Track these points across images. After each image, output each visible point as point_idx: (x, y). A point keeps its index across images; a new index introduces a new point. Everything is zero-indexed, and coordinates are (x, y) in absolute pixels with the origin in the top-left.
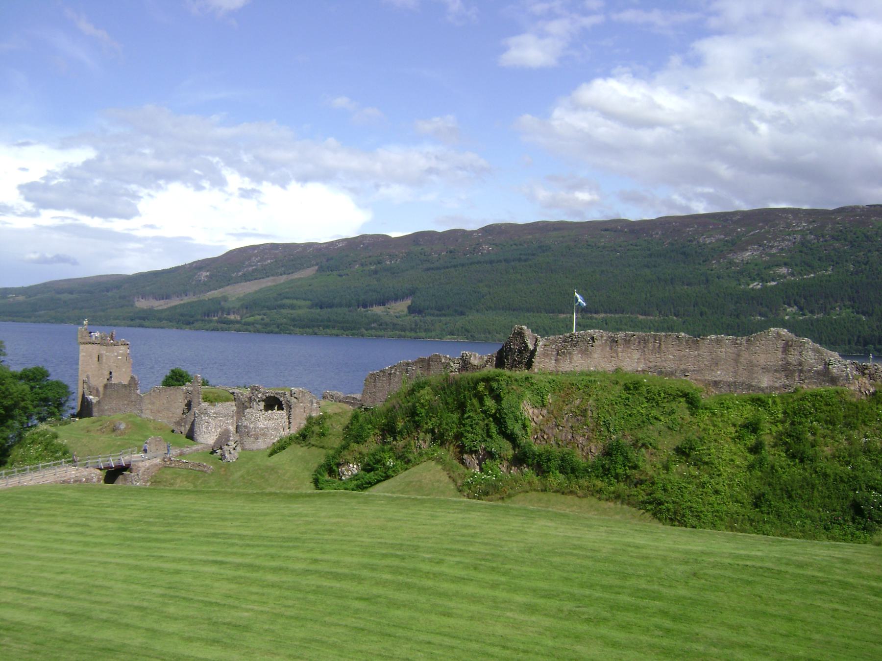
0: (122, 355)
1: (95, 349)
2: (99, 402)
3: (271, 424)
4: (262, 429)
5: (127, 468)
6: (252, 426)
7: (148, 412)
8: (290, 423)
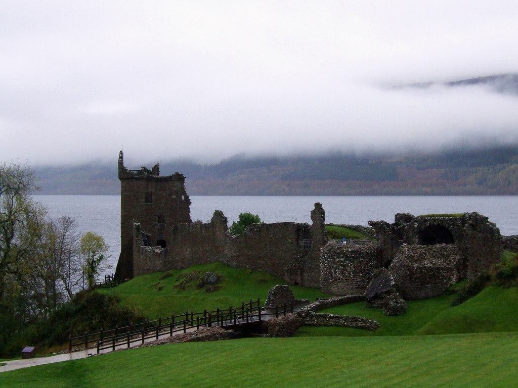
3: (440, 263)
4: (431, 269)
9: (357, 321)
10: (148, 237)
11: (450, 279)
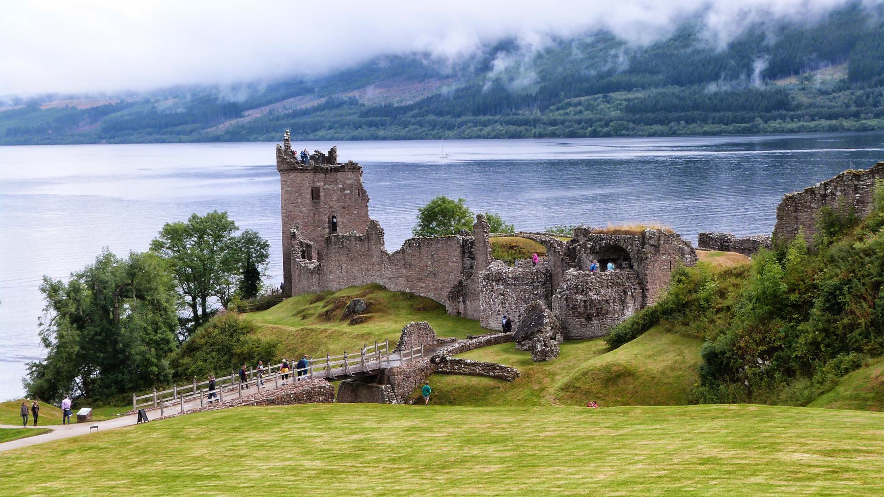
0: (351, 187)
2: (319, 269)
9: (495, 368)
10: (308, 246)
11: (623, 314)
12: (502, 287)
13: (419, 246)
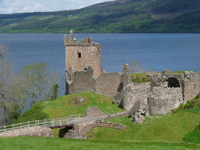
0: (93, 52)
1: (75, 50)
2: (72, 84)
5: (71, 127)
6: (157, 98)
7: (99, 90)
8: (184, 96)
12: (130, 93)
13: (105, 76)
